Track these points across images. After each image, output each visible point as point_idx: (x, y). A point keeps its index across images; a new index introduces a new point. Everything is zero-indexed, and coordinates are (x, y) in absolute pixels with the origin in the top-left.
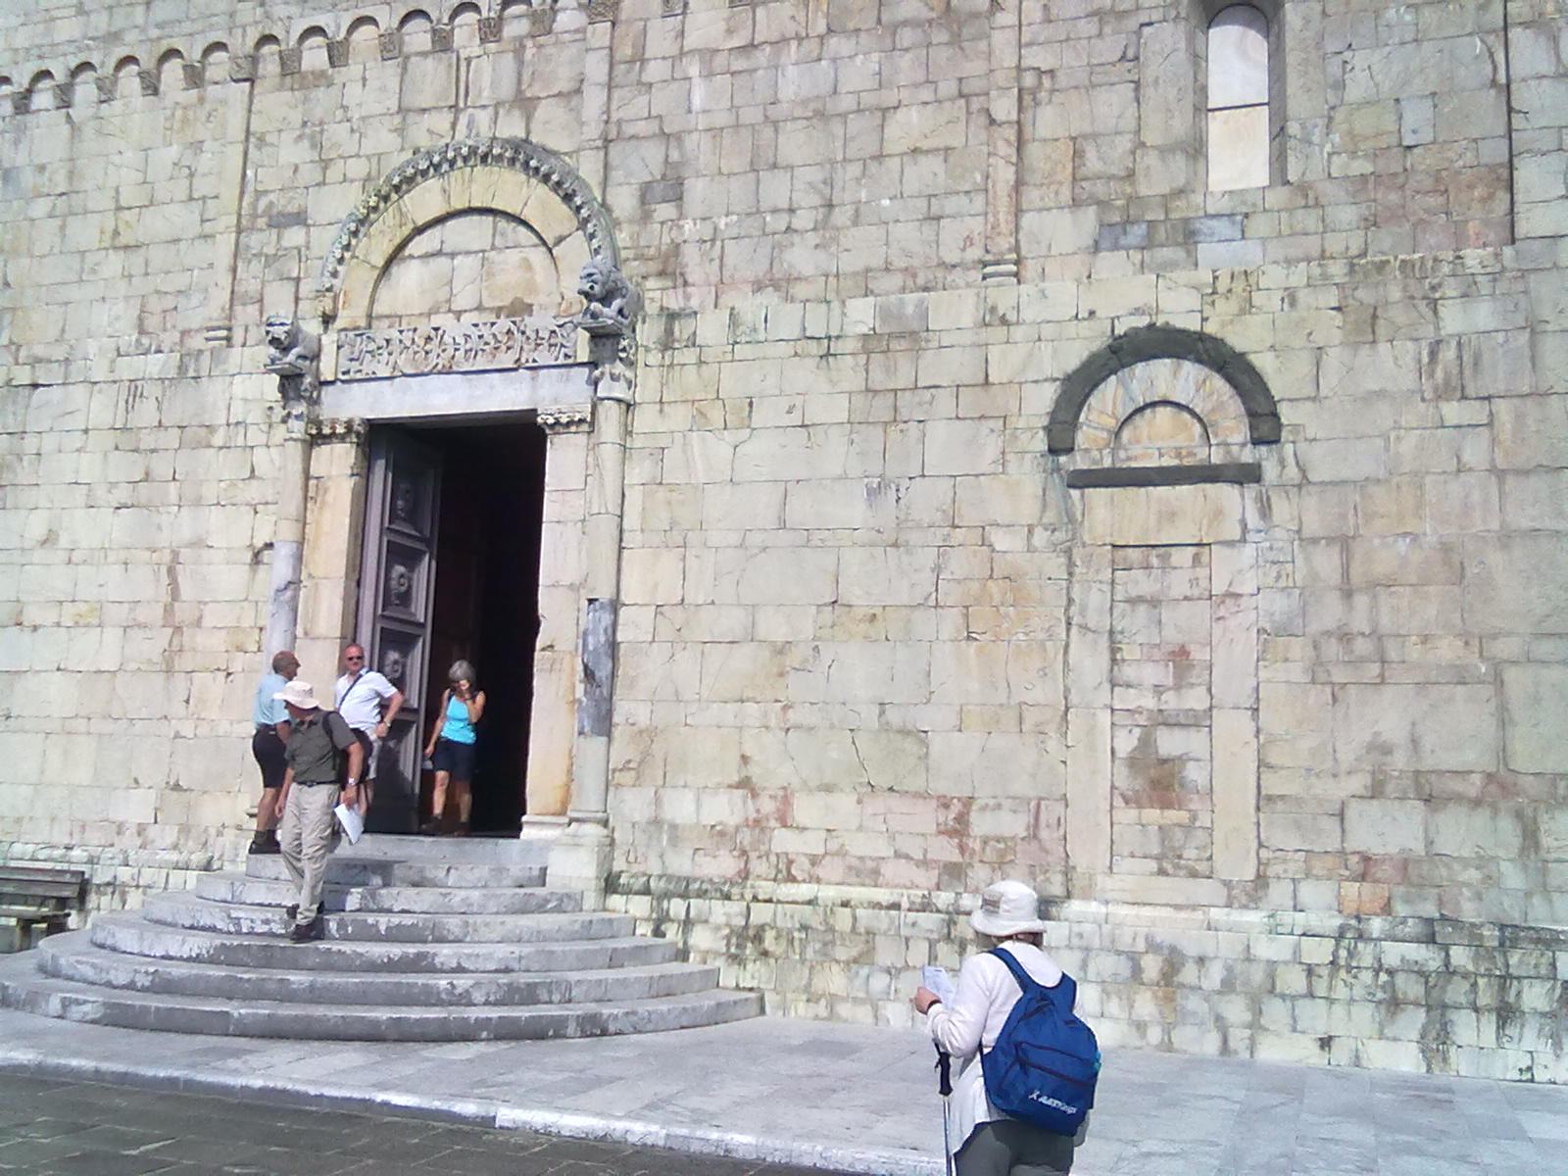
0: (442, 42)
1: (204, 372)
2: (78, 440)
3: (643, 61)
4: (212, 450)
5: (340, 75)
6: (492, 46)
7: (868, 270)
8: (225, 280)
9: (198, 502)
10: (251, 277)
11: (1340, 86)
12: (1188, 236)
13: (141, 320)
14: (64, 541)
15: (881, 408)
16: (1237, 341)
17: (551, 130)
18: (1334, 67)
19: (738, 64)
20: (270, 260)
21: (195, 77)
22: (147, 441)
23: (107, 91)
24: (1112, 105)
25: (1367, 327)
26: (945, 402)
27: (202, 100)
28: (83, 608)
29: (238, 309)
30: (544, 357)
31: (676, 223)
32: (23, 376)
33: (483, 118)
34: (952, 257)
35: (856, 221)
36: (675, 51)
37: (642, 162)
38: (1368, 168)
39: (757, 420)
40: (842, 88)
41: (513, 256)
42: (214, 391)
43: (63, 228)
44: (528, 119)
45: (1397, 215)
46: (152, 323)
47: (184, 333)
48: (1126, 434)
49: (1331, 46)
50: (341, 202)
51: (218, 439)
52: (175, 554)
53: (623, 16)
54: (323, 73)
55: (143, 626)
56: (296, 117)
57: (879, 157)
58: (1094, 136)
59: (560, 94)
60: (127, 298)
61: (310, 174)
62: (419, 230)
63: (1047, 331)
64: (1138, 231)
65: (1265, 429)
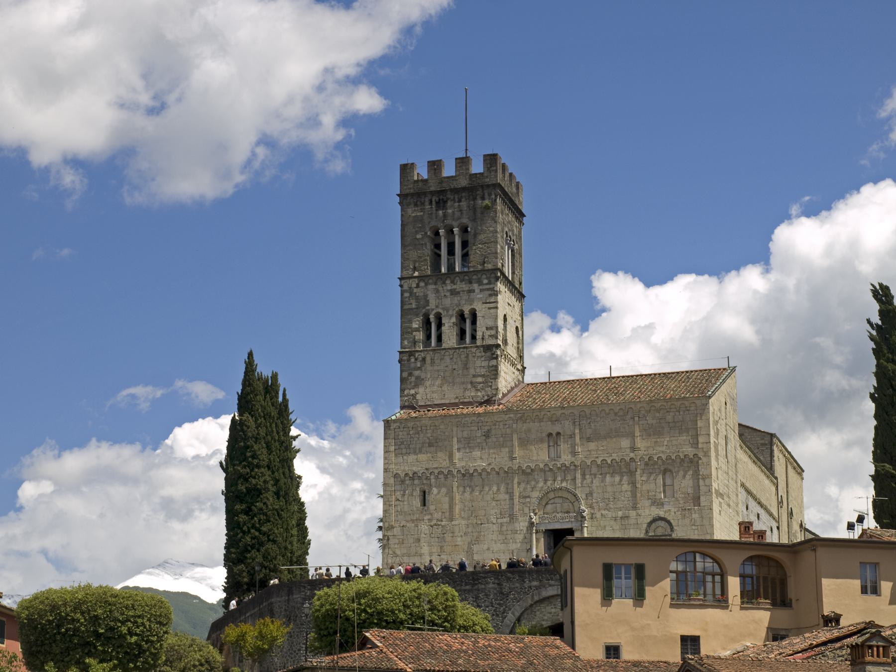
14: (491, 549)
16: (669, 519)
25: (684, 517)
27: (508, 476)
41: (566, 504)
42: (517, 525)
51: (518, 532)
57: (622, 492)
62: (550, 500)
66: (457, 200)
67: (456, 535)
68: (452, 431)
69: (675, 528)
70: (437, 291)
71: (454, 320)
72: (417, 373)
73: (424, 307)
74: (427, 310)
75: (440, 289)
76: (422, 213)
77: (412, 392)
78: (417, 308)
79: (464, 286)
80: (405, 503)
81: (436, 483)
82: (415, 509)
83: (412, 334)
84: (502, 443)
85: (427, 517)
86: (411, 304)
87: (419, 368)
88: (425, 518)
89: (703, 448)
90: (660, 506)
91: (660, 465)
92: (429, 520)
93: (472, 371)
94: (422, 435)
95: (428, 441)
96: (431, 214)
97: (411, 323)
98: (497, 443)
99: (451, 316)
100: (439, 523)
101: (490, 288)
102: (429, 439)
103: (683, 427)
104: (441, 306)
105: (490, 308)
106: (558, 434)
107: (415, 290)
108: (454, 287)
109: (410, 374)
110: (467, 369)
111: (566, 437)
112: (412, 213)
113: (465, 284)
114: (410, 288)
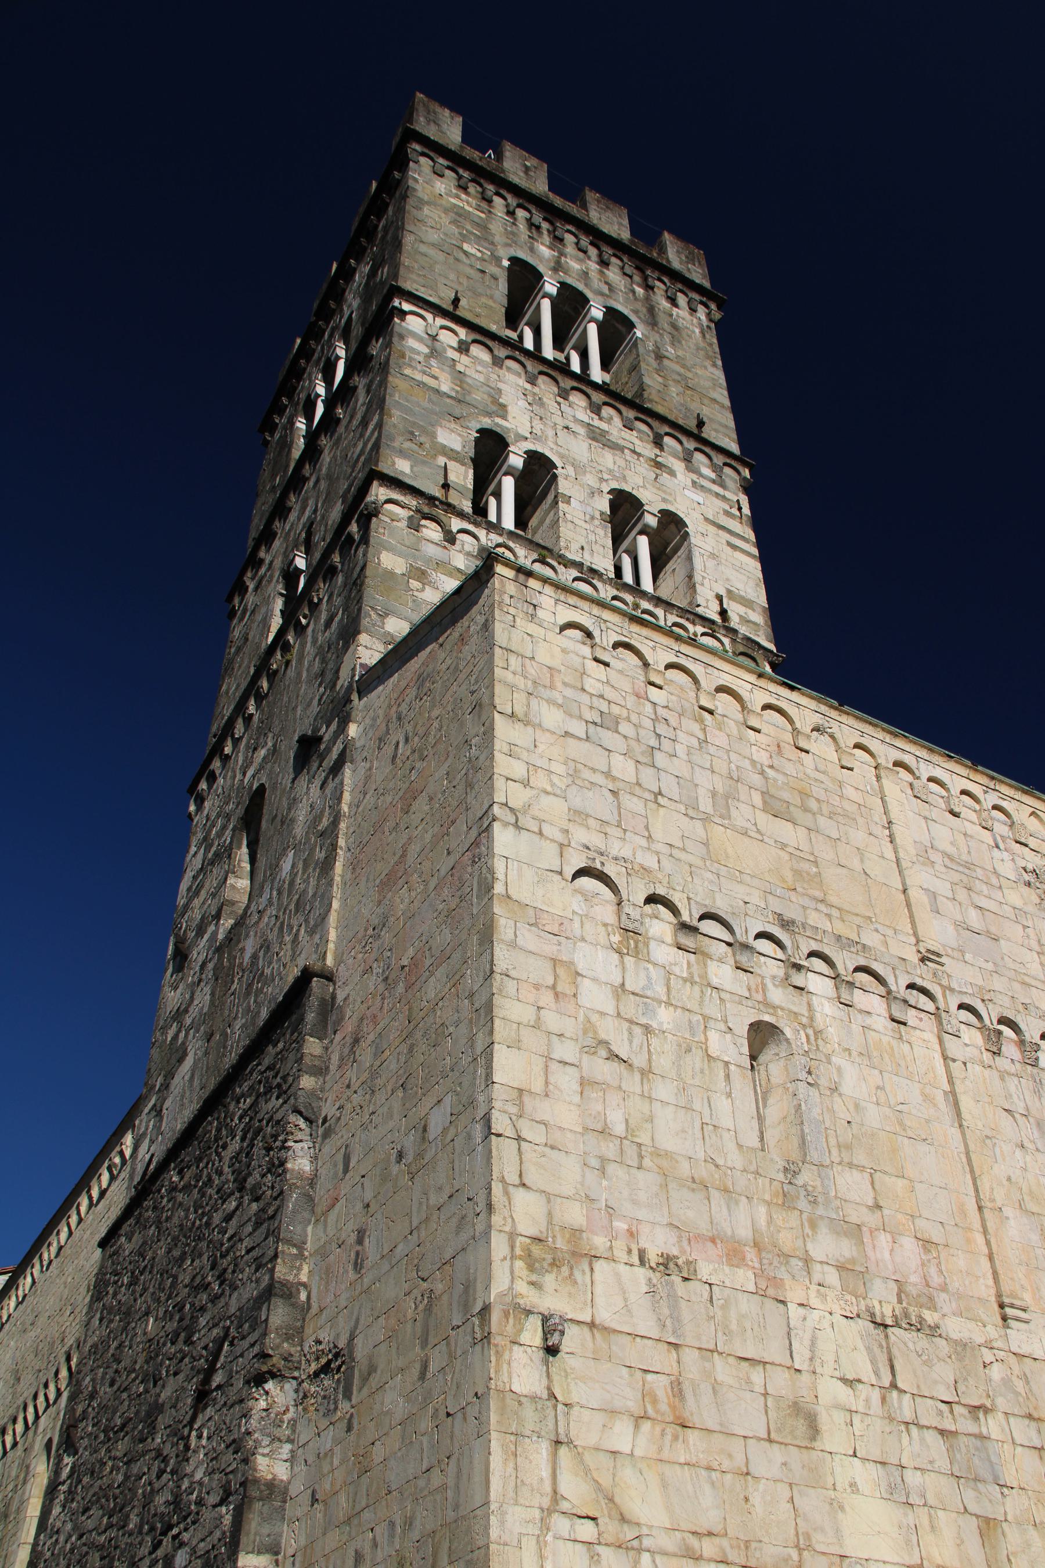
82: (735, 1159)
95: (756, 779)
102: (762, 773)
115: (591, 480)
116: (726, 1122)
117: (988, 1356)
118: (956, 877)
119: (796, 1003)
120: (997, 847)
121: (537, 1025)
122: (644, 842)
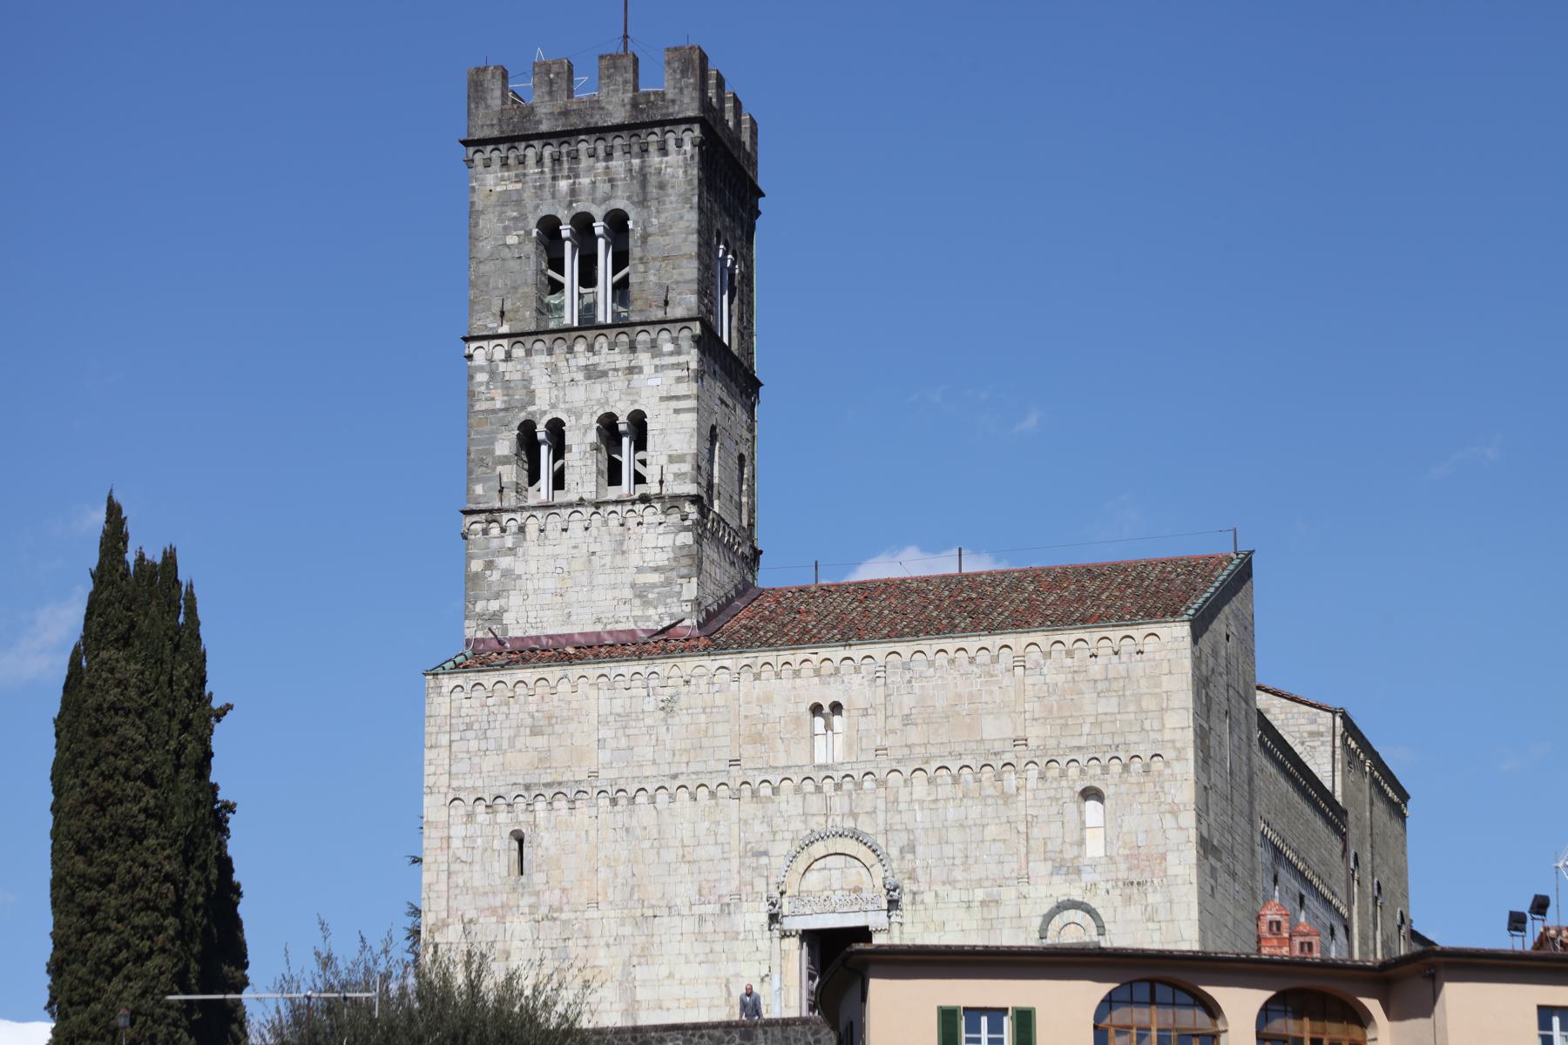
0: (819, 789)
1: (732, 911)
2: (679, 938)
3: (898, 802)
4: (739, 942)
5: (777, 799)
6: (839, 793)
7: (981, 879)
8: (737, 877)
9: (735, 960)
10: (747, 874)
11: (1121, 827)
12: (1078, 871)
13: (700, 891)
14: (677, 976)
15: (988, 925)
16: (1093, 905)
17: (865, 826)
18: (1119, 820)
19: (933, 806)
20: (754, 869)
21: (713, 795)
22: (710, 938)
23: (672, 798)
24: (1055, 828)
25: (1128, 900)
26: (1007, 922)
27: (717, 804)
28: (689, 1001)
29: (743, 887)
30: (870, 907)
31: (914, 861)
32: (650, 913)
33: (838, 819)
34: (1007, 875)
35: (976, 863)
36: (909, 799)
37: (902, 839)
38: (1129, 852)
39: (947, 928)
40: (969, 817)
41: (854, 871)
43: (658, 853)
44: (856, 820)
45: (1137, 867)
46: (705, 892)
47: (720, 896)
48: (1062, 932)
49: (1118, 814)
50: (782, 849)
52: (728, 980)
53: (889, 785)
54: (770, 798)
55: (717, 1006)
56: (760, 814)
57: (982, 841)
58: (1050, 838)
59: (867, 813)
60: (692, 882)
61: (768, 837)
62: (816, 860)
63: (1038, 900)
64: (1064, 870)
65: (1101, 931)
66: (601, 153)
67: (594, 941)
68: (587, 698)
69: (1107, 926)
70: (554, 370)
71: (593, 436)
72: (504, 562)
73: (523, 408)
74: (530, 413)
75: (562, 364)
76: (519, 186)
77: (494, 605)
78: (506, 410)
79: (620, 359)
80: (477, 867)
81: (549, 821)
82: (498, 881)
83: (494, 469)
84: (703, 727)
85: (526, 901)
86: (493, 399)
87: (512, 551)
88: (521, 903)
89: (1173, 741)
90: (1073, 877)
91: (1074, 781)
92: (530, 906)
93: (634, 559)
94: (515, 708)
95: (529, 721)
96: (541, 187)
97: (493, 444)
98: (692, 726)
99: (587, 429)
100: (555, 915)
101: (679, 364)
102: (533, 717)
103: (1128, 693)
104: (562, 406)
105: (677, 411)
106: (836, 708)
107: (502, 367)
108: (595, 360)
109: (490, 565)
110: (623, 552)
111: (854, 713)
112: (496, 185)
113: (621, 353)
114: (491, 361)
115: (585, 420)
116: (497, 870)
117: (575, 922)
118: (619, 724)
119: (530, 818)
120: (648, 695)
121: (436, 861)
122: (478, 775)
